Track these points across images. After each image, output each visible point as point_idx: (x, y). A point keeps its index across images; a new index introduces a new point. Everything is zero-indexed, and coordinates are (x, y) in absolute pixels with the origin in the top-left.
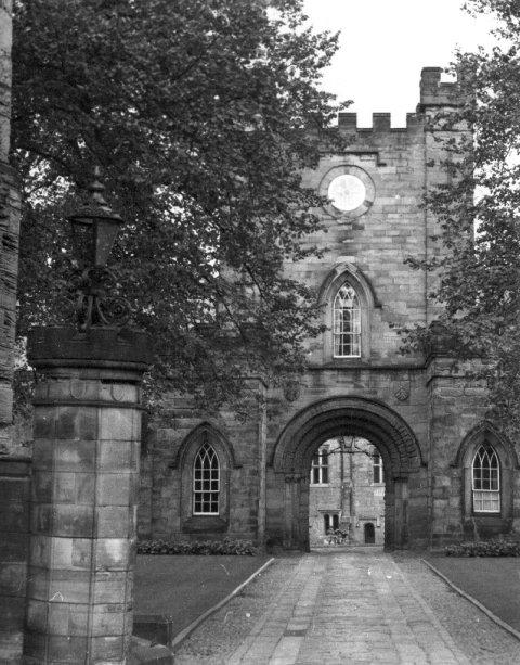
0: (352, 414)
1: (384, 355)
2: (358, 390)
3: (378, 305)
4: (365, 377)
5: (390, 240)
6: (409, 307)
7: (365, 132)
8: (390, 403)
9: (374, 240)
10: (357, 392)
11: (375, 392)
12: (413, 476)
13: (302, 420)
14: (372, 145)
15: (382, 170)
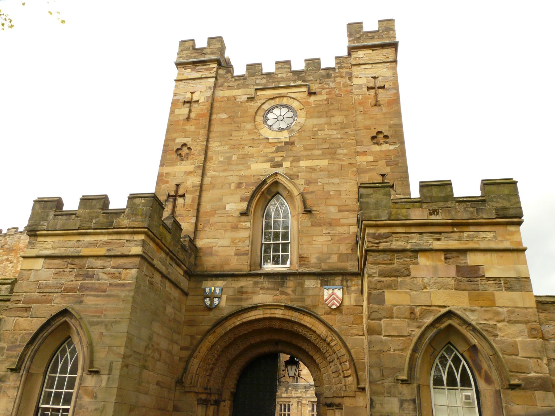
0: (277, 325)
1: (313, 260)
2: (283, 297)
3: (308, 211)
4: (291, 283)
5: (320, 152)
6: (340, 211)
7: (297, 73)
8: (320, 312)
9: (305, 153)
10: (283, 300)
11: (303, 300)
12: (347, 402)
13: (221, 331)
14: (303, 81)
15: (312, 99)
